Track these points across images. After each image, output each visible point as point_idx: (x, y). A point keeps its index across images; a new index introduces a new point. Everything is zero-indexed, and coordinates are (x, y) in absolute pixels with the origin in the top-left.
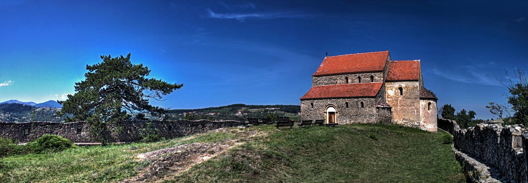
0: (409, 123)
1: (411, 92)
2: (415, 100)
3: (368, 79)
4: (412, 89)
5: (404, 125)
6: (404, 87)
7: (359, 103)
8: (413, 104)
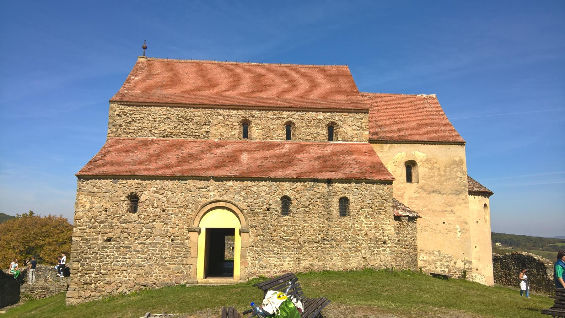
0: (439, 263)
2: (455, 197)
4: (446, 167)
5: (425, 267)
6: (422, 161)
8: (449, 209)
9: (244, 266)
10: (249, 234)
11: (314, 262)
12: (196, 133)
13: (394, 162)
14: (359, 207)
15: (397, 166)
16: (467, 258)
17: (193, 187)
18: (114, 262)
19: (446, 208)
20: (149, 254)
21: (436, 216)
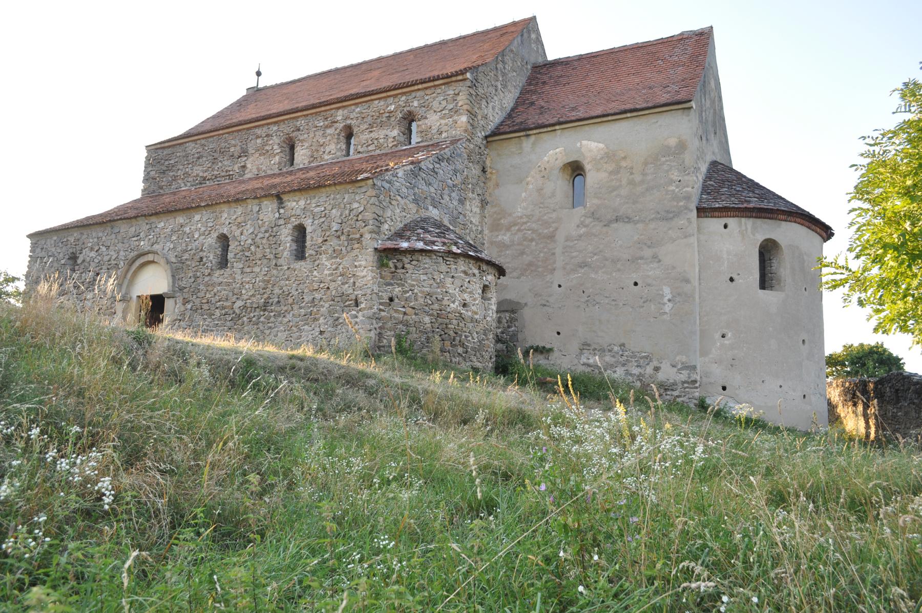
1: (638, 178)
3: (388, 132)
4: (646, 163)
7: (286, 236)
8: (647, 253)
10: (176, 301)
13: (541, 171)
14: (320, 240)
15: (546, 177)
16: (684, 359)
19: (642, 251)
21: (619, 270)
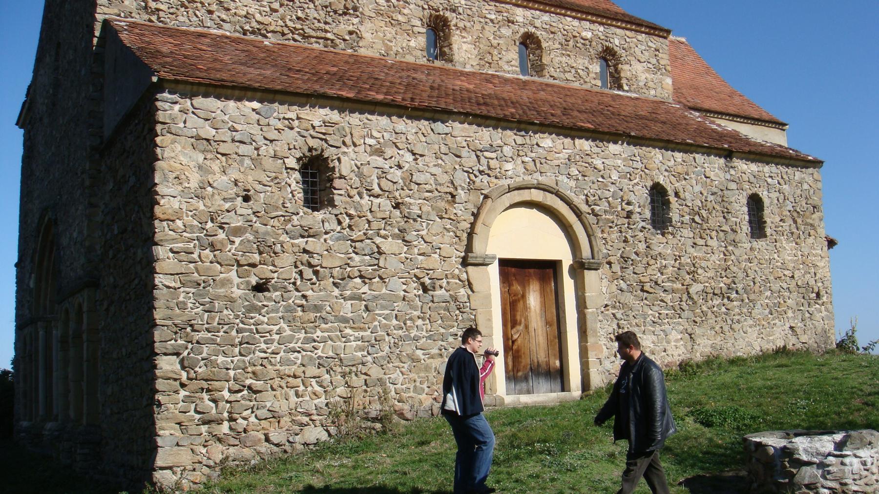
9: (596, 355)
11: (718, 340)
12: (326, 31)
17: (464, 144)
18: (282, 354)
20: (375, 326)
